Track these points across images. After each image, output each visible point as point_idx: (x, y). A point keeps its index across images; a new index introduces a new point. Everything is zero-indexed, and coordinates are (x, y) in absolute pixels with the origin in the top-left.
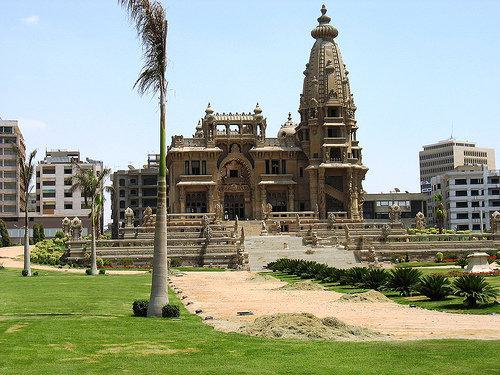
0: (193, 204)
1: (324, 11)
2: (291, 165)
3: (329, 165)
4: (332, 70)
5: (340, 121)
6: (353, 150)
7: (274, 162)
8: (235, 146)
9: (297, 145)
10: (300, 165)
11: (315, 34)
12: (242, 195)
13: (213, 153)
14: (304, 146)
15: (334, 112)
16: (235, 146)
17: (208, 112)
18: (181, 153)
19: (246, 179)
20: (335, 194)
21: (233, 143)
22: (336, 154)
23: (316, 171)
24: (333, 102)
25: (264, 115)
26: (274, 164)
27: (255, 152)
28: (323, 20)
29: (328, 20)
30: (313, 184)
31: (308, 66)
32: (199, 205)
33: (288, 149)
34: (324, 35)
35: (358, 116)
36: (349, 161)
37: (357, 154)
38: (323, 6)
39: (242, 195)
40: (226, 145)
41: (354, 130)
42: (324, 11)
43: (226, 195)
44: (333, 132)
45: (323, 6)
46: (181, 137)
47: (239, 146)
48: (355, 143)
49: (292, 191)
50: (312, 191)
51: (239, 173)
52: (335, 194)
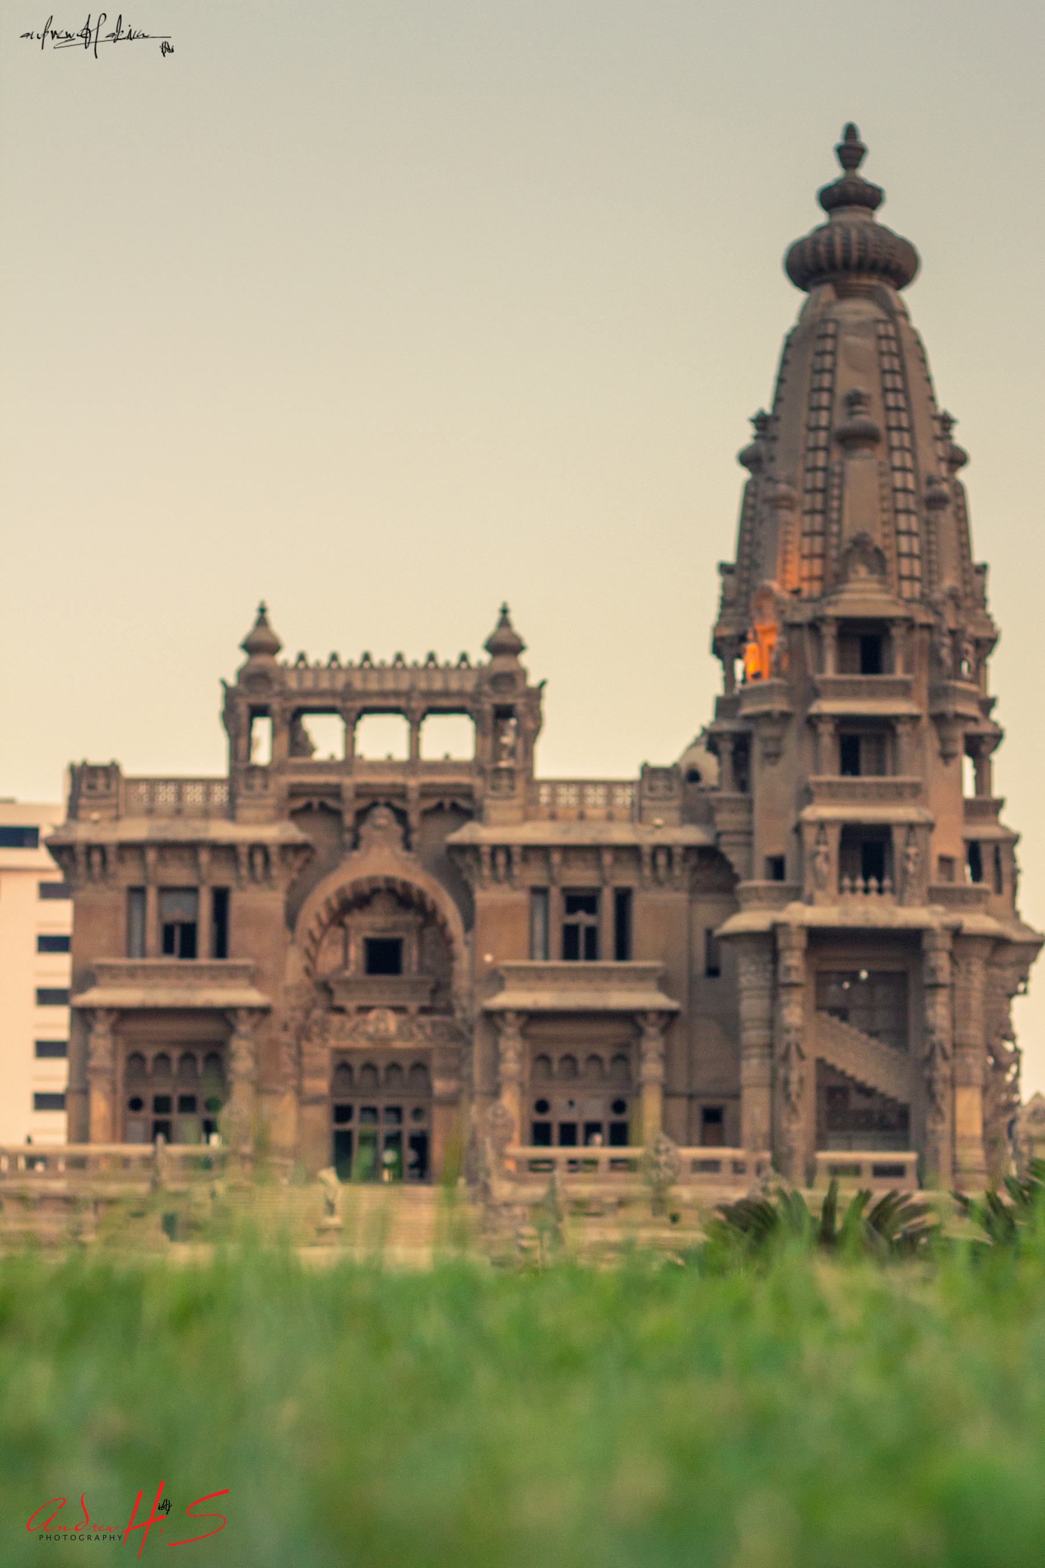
0: (162, 1104)
1: (851, 152)
2: (663, 914)
3: (823, 913)
4: (868, 437)
5: (905, 690)
6: (973, 850)
7: (581, 901)
8: (382, 817)
9: (689, 815)
10: (705, 912)
11: (806, 266)
12: (420, 1067)
13: (258, 847)
14: (726, 819)
15: (867, 644)
16: (382, 817)
17: (250, 647)
18: (102, 848)
19: (438, 995)
20: (863, 1060)
21: (372, 800)
22: (868, 853)
23: (769, 941)
24: (864, 597)
25: (534, 665)
26: (587, 921)
27: (473, 849)
28: (849, 196)
29: (872, 198)
30: (752, 1006)
31: (761, 422)
32: (188, 1104)
33: (647, 837)
34: (850, 260)
35: (1000, 674)
36: (935, 896)
37: (990, 860)
38: (851, 131)
39: (420, 1067)
40: (330, 807)
41: (981, 746)
42: (851, 152)
43: (343, 1067)
44: (861, 745)
45: (851, 131)
46: (111, 771)
47: (401, 816)
48: (986, 807)
49: (652, 1045)
50: (753, 1035)
51: (411, 956)
52: (863, 1060)
